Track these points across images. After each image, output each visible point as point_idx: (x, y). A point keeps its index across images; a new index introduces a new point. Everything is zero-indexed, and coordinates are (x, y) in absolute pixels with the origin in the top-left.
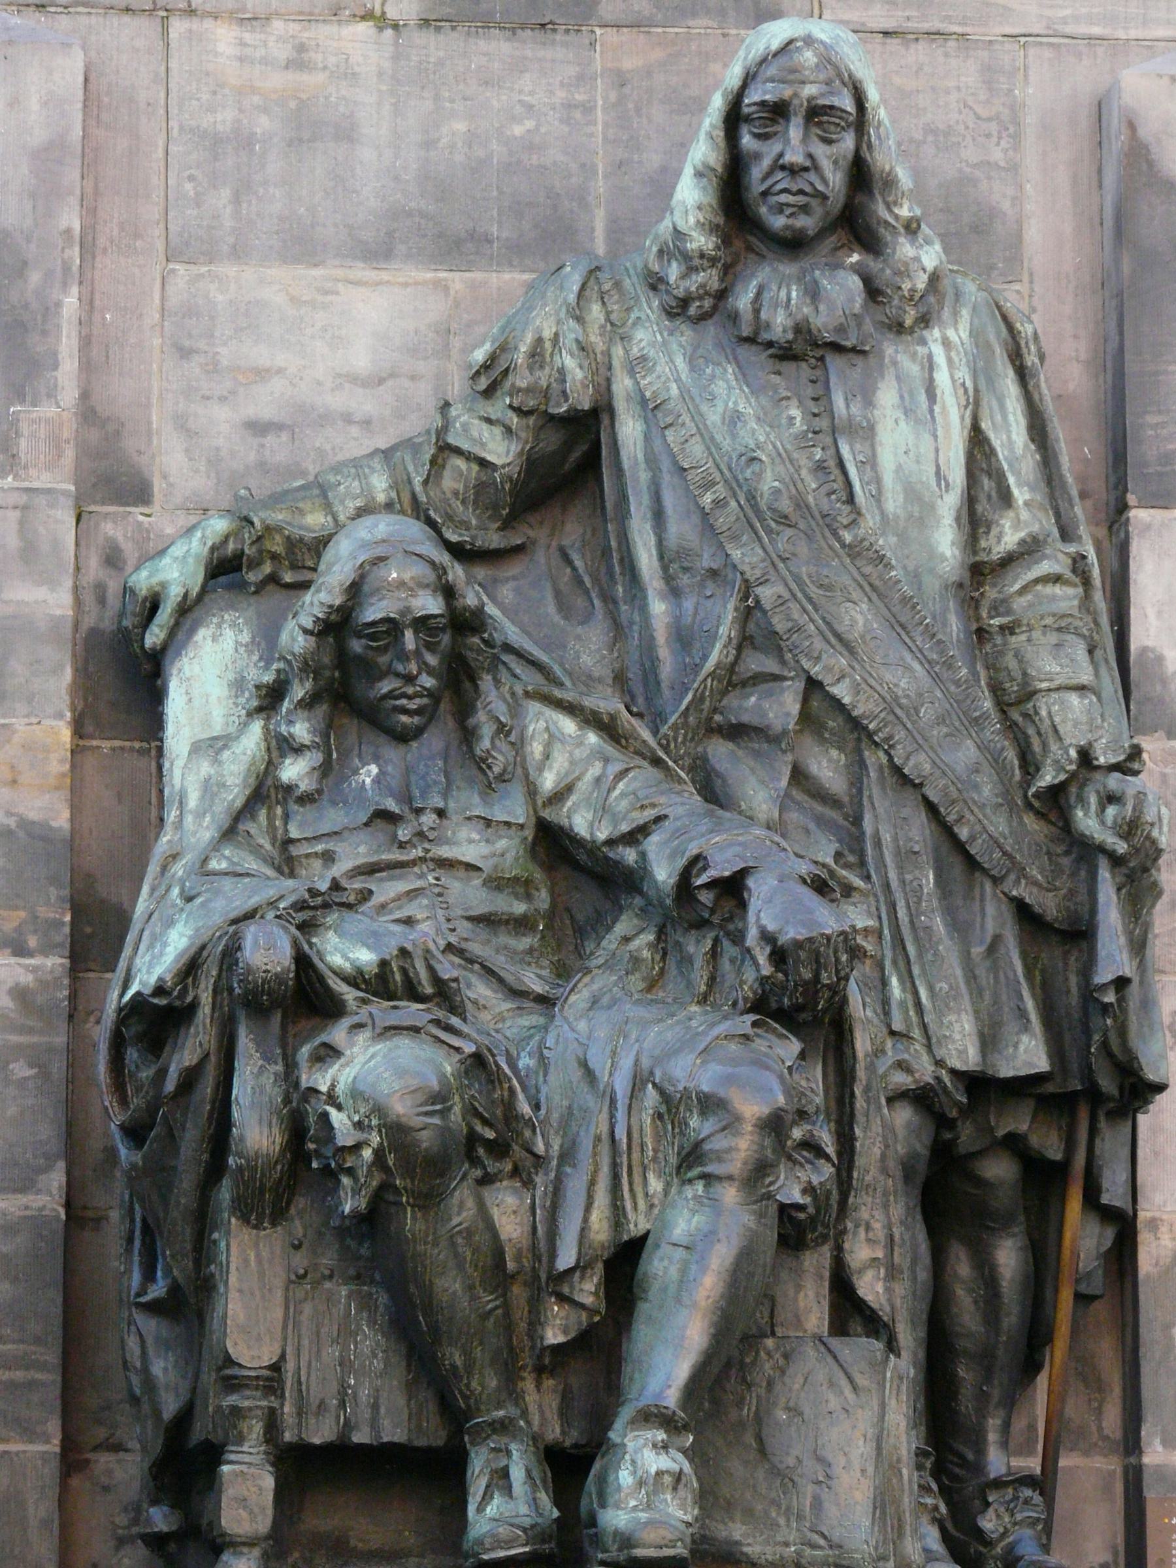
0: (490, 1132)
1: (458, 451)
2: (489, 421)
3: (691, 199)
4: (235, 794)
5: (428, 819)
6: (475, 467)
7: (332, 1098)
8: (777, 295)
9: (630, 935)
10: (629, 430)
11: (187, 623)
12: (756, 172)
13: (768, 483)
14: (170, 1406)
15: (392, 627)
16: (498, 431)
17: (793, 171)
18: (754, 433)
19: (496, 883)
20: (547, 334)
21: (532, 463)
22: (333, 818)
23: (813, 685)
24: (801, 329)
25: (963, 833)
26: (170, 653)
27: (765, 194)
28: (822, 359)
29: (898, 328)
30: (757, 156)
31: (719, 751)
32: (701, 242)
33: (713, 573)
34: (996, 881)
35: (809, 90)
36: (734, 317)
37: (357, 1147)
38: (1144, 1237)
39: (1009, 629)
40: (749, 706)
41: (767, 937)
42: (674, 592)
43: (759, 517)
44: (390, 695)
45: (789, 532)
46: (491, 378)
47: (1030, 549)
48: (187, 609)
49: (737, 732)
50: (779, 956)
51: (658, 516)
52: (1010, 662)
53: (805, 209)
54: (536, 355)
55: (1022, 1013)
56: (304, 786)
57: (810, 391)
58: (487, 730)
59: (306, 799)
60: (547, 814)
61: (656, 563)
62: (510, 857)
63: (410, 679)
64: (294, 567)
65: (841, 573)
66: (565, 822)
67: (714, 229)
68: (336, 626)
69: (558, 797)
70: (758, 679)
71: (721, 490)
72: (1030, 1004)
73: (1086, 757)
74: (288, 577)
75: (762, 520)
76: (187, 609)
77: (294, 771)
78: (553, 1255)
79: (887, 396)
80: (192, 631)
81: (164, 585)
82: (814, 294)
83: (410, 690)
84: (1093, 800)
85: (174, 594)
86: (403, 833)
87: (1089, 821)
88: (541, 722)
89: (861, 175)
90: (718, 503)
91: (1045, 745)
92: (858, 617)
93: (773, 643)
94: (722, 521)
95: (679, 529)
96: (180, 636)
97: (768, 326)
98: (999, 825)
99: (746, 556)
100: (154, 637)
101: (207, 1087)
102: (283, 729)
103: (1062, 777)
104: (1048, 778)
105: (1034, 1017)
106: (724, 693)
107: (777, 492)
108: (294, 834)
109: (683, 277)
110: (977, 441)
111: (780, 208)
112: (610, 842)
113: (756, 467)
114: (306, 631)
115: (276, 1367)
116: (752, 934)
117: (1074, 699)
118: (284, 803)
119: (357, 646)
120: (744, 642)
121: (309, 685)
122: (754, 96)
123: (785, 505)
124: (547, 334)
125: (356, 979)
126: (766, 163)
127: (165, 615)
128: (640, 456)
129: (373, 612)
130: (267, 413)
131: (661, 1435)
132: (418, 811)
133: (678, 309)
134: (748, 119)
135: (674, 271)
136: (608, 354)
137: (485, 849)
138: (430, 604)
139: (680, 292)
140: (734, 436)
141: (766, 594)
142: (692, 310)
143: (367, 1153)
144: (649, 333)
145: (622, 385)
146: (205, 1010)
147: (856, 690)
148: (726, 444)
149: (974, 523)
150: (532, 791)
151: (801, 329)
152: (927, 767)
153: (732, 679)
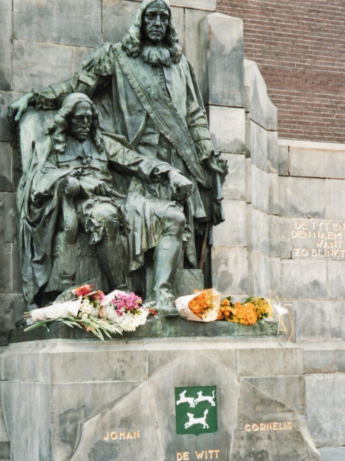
0: (120, 225)
1: (82, 82)
2: (89, 76)
3: (134, 32)
4: (47, 151)
5: (89, 159)
6: (86, 86)
7: (91, 216)
8: (154, 53)
9: (134, 185)
10: (120, 80)
11: (24, 116)
12: (148, 27)
13: (153, 92)
14: (41, 284)
15: (82, 117)
16: (91, 79)
17: (157, 26)
18: (148, 82)
19: (103, 173)
20: (102, 58)
21: (98, 86)
22: (68, 158)
23: (162, 136)
24: (159, 60)
25: (189, 167)
26: (20, 122)
27: (151, 31)
28: (162, 68)
29: (175, 63)
30: (149, 23)
31: (141, 148)
32: (137, 41)
33: (140, 111)
34: (194, 177)
35: (162, 10)
36: (143, 57)
37: (99, 227)
38: (212, 251)
39: (195, 126)
40: (146, 139)
41: (176, 185)
42: (130, 114)
43: (150, 99)
44: (81, 132)
45: (157, 103)
46: (89, 67)
47: (197, 111)
48: (24, 112)
49: (146, 145)
50: (178, 189)
51: (127, 99)
52: (196, 134)
53: (159, 35)
54: (100, 62)
55: (200, 205)
56: (62, 150)
57: (159, 74)
58: (99, 141)
59: (62, 153)
60: (112, 159)
61: (126, 108)
62: (105, 168)
63: (85, 128)
64: (46, 105)
65: (168, 112)
66: (116, 161)
67: (139, 38)
68: (69, 117)
69: (114, 155)
70: (150, 133)
71: (142, 93)
72: (201, 203)
73: (213, 153)
74: (45, 107)
75: (151, 100)
76: (24, 112)
77: (59, 147)
78: (134, 251)
79: (173, 75)
80: (25, 118)
81: (19, 107)
82: (161, 53)
83: (85, 131)
84: (215, 162)
85: (21, 109)
86: (85, 161)
87: (215, 166)
88: (108, 140)
89: (169, 30)
90: (141, 96)
91: (203, 151)
92: (171, 122)
93: (153, 126)
94: (142, 100)
95: (132, 101)
96: (23, 118)
97: (151, 59)
98: (196, 166)
99: (147, 107)
100: (17, 118)
101: (54, 215)
102: (56, 138)
103: (208, 157)
104: (204, 157)
105: (203, 206)
106: (142, 136)
107: (154, 94)
108: (60, 160)
109: (132, 48)
110: (188, 87)
111: (154, 35)
112: (129, 165)
113: (150, 89)
114: (63, 117)
115: (74, 275)
116: (172, 185)
117: (208, 141)
118: (56, 154)
119: (74, 121)
120: (146, 125)
121: (62, 129)
122: (149, 10)
123: (156, 97)
124: (102, 58)
125: (91, 191)
126: (151, 25)
127: (19, 113)
128: (122, 86)
129: (78, 114)
130: (34, 73)
131: (167, 289)
132: (87, 157)
133: (130, 55)
134: (147, 15)
135: (130, 46)
136: (114, 63)
137: (100, 166)
138: (89, 112)
139: (132, 51)
140: (144, 81)
141: (152, 115)
142: (134, 55)
143: (102, 228)
144: (123, 59)
145: (118, 70)
146: (56, 197)
147: (171, 136)
148: (143, 83)
149: (188, 105)
150: (107, 154)
151: (159, 60)
152: (184, 153)
153: (144, 133)
